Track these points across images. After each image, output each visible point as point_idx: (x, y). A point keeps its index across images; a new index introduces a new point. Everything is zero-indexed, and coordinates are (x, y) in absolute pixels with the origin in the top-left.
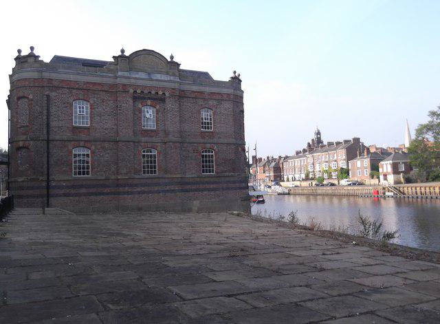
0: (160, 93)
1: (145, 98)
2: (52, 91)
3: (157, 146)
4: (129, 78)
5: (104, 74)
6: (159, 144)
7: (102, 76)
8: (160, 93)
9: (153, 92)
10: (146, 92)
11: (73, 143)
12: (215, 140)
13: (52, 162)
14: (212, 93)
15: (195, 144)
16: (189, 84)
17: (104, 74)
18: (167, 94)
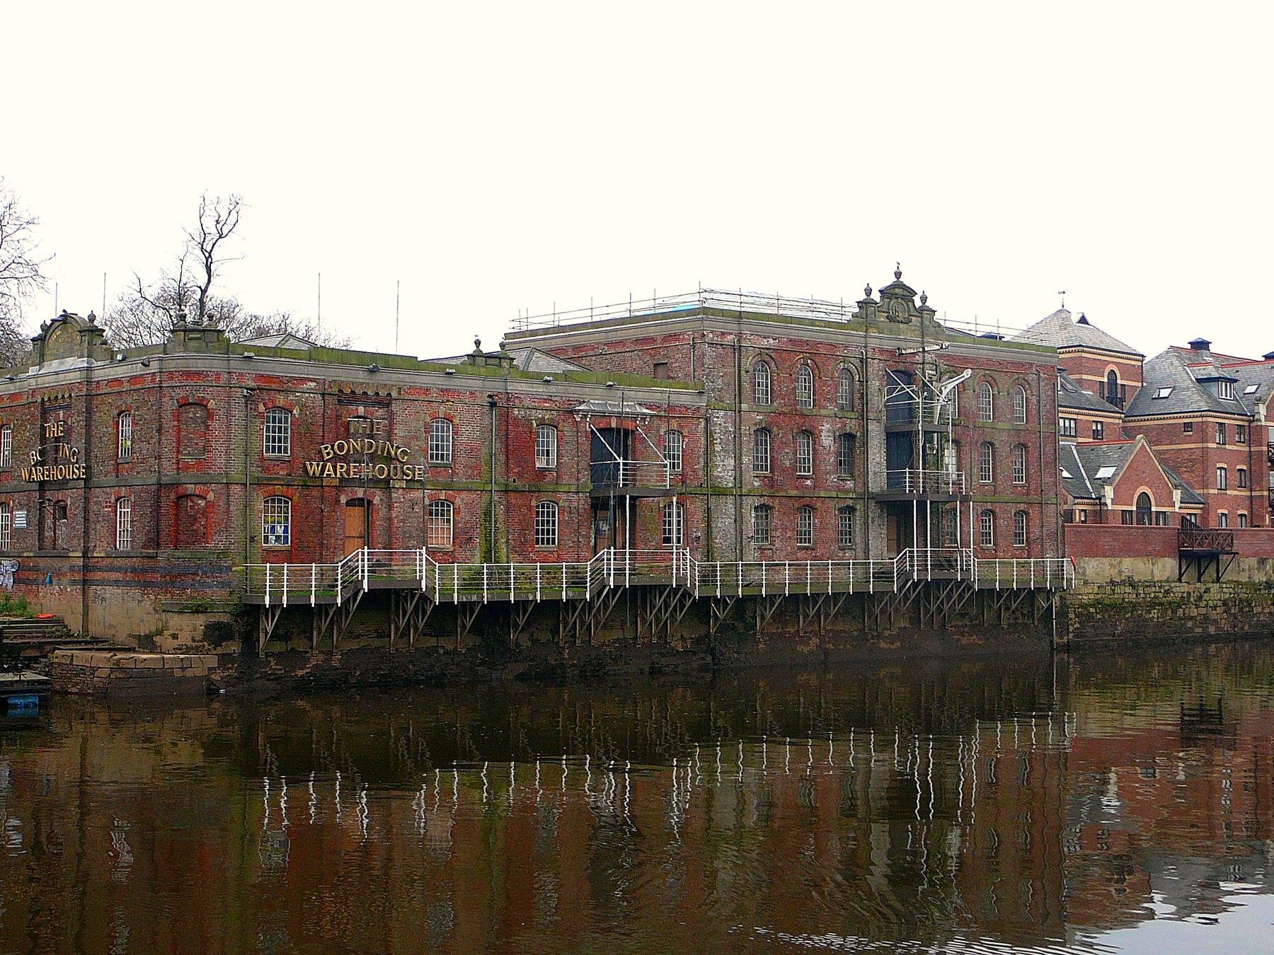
15: (108, 490)
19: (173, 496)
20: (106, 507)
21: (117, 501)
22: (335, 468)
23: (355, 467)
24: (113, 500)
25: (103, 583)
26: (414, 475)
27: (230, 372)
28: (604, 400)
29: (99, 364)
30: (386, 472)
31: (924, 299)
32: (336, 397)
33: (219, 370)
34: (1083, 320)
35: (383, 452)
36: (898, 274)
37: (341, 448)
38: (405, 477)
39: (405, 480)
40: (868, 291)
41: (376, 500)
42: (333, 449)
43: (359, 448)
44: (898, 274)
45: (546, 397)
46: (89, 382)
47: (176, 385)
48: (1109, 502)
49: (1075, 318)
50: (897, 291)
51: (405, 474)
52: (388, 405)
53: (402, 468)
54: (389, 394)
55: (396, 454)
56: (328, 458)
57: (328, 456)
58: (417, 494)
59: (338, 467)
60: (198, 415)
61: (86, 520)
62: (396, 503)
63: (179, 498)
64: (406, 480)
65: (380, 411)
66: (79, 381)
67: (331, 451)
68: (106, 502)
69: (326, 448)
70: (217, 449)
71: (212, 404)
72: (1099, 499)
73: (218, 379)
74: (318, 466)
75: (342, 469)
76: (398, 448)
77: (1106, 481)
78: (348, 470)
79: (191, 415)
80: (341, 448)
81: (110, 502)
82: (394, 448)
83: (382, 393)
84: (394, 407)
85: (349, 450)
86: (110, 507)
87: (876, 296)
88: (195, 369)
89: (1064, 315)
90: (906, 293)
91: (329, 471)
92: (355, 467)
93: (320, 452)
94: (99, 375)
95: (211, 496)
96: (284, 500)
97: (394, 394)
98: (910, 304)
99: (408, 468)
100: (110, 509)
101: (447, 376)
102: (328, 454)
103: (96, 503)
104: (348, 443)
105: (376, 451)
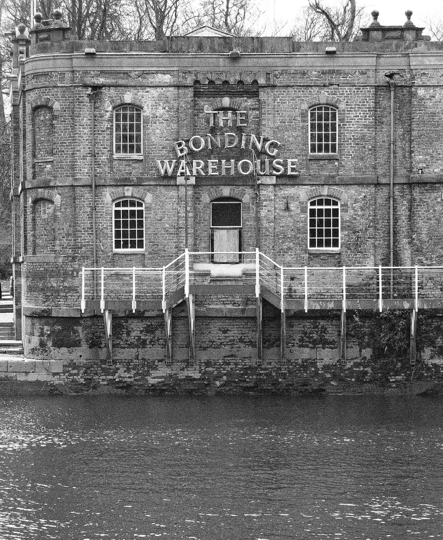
26: (286, 170)
27: (73, 72)
32: (191, 89)
33: (63, 69)
38: (274, 172)
52: (255, 94)
53: (271, 163)
54: (255, 82)
55: (263, 147)
57: (181, 153)
58: (290, 191)
59: (194, 164)
60: (47, 117)
62: (266, 201)
65: (249, 100)
67: (186, 148)
70: (63, 151)
71: (57, 106)
73: (62, 79)
74: (170, 163)
78: (206, 166)
79: (42, 118)
82: (262, 140)
83: (249, 80)
84: (263, 96)
85: (206, 146)
88: (41, 71)
91: (183, 169)
95: (57, 199)
96: (137, 202)
97: (262, 81)
99: (278, 163)
101: (329, 56)
102: (182, 151)
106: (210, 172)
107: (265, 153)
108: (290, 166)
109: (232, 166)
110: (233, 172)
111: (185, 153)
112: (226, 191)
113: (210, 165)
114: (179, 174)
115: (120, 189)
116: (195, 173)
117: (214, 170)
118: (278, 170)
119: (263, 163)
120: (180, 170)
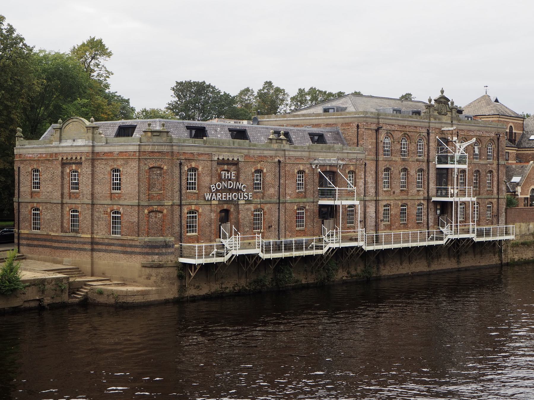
0: (79, 158)
1: (70, 164)
2: (21, 163)
3: (78, 207)
4: (58, 147)
5: (48, 145)
6: (80, 205)
7: (46, 147)
8: (79, 158)
9: (74, 158)
10: (69, 158)
11: (31, 204)
12: (121, 202)
13: (21, 219)
14: (121, 152)
15: (106, 206)
16: (102, 146)
17: (48, 145)
18: (83, 159)
19: (146, 211)
20: (104, 214)
21: (111, 211)
22: (216, 194)
23: (224, 195)
24: (109, 210)
25: (99, 251)
28: (324, 158)
29: (99, 144)
30: (237, 196)
31: (452, 103)
34: (497, 101)
35: (236, 187)
36: (442, 92)
37: (219, 186)
38: (245, 198)
39: (245, 200)
40: (430, 100)
41: (232, 210)
42: (215, 187)
43: (226, 186)
44: (442, 92)
45: (300, 158)
46: (93, 152)
47: (148, 158)
48: (519, 194)
49: (493, 100)
50: (442, 100)
51: (244, 197)
56: (213, 191)
59: (218, 195)
61: (92, 220)
62: (241, 211)
63: (149, 212)
64: (245, 200)
65: (233, 167)
66: (87, 151)
68: (104, 212)
69: (213, 186)
72: (515, 192)
74: (210, 194)
75: (219, 196)
76: (242, 185)
77: (518, 184)
80: (219, 186)
81: (107, 212)
86: (107, 214)
87: (433, 102)
89: (487, 98)
90: (445, 101)
92: (224, 195)
93: (210, 188)
94: (97, 149)
95: (165, 211)
98: (447, 106)
100: (107, 215)
103: (97, 212)
104: (221, 183)
105: (233, 187)
106: (223, 199)
107: (241, 190)
108: (250, 196)
109: (231, 196)
110: (231, 199)
111: (215, 190)
112: (225, 207)
113: (223, 195)
114: (212, 199)
115: (190, 206)
116: (218, 199)
117: (225, 198)
118: (246, 198)
119: (241, 194)
120: (213, 198)
